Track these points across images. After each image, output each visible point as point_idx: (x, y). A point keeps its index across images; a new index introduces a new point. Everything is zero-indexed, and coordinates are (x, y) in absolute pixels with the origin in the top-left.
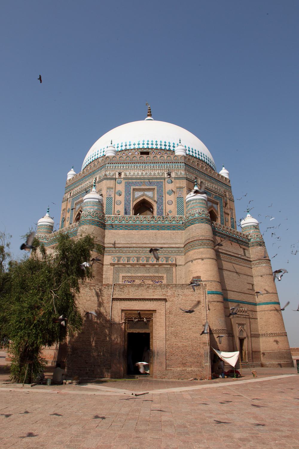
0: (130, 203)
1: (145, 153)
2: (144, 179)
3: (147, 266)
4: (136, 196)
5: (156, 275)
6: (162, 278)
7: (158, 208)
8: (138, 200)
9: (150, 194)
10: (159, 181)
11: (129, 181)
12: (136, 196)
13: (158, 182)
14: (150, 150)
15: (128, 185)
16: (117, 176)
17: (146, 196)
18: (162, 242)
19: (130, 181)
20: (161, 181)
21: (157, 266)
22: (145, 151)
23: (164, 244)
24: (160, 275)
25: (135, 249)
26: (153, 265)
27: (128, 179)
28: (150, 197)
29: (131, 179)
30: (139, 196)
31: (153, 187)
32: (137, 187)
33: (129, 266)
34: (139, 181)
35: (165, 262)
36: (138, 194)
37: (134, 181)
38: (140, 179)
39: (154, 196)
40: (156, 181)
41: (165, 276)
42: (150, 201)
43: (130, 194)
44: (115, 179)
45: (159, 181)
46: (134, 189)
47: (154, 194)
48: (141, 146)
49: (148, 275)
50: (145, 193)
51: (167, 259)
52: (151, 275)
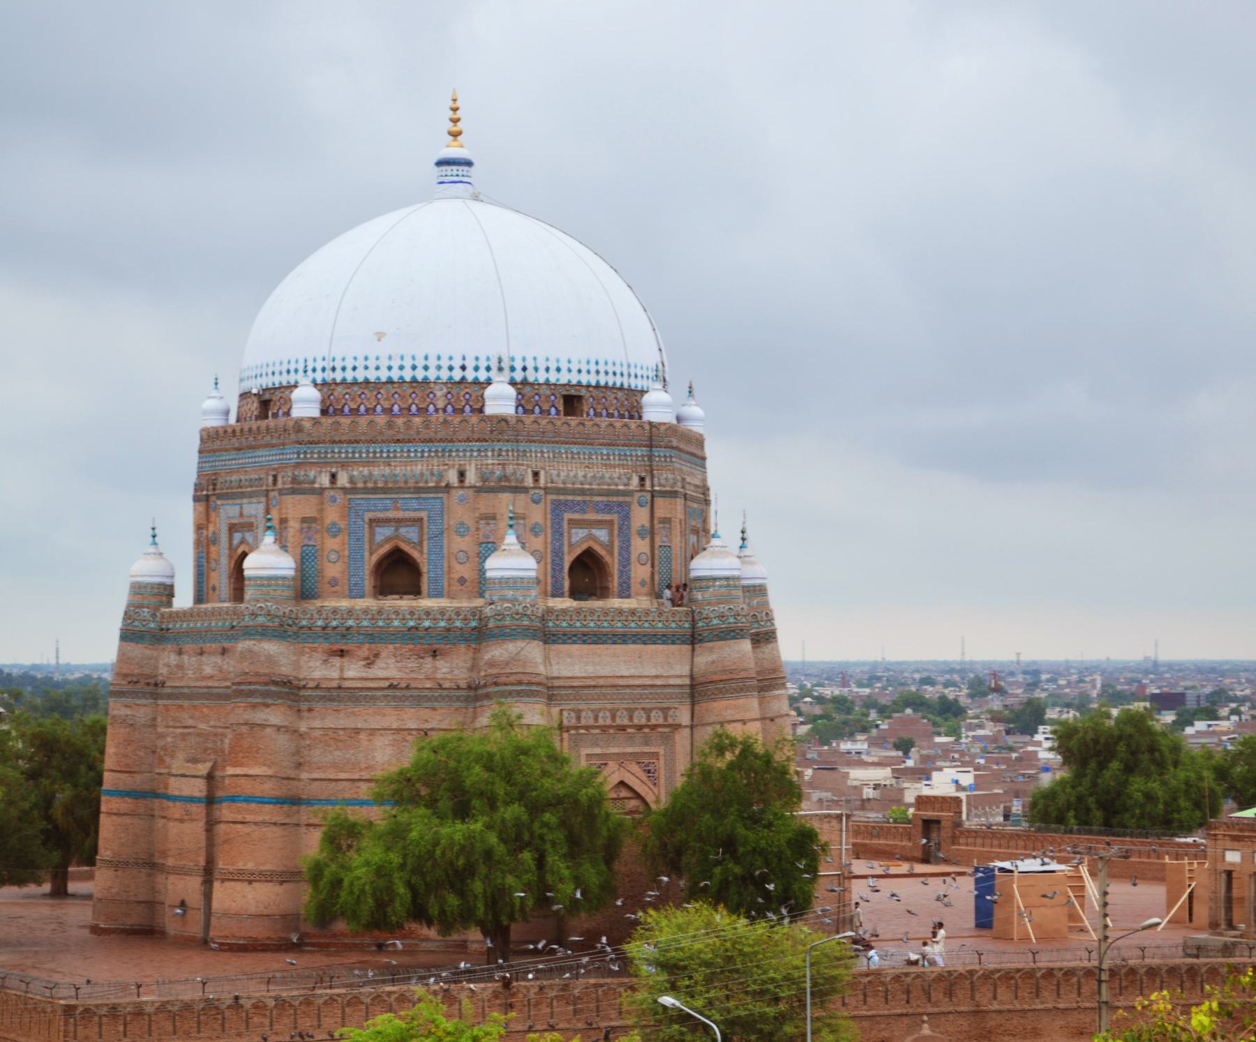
0: (562, 559)
1: (572, 401)
2: (591, 492)
3: (629, 730)
4: (574, 540)
5: (646, 749)
6: (655, 755)
7: (621, 573)
8: (578, 551)
9: (602, 534)
10: (621, 499)
11: (565, 502)
12: (574, 540)
13: (620, 504)
14: (583, 392)
15: (558, 508)
16: (529, 481)
17: (595, 539)
18: (653, 672)
19: (562, 497)
20: (627, 499)
21: (647, 730)
22: (573, 392)
23: (657, 677)
24: (653, 750)
25: (604, 691)
26: (640, 728)
27: (559, 491)
28: (601, 544)
29: (564, 491)
30: (578, 539)
31: (607, 517)
32: (577, 516)
33: (597, 731)
34: (579, 498)
35: (661, 721)
36: (579, 534)
37: (570, 498)
38: (582, 492)
39: (612, 542)
40: (615, 499)
41: (661, 751)
42: (602, 552)
43: (562, 535)
44: (525, 490)
45: (621, 499)
46: (571, 521)
47: (611, 534)
48: (564, 378)
49: (630, 750)
50: (594, 531)
51: (665, 711)
52: (637, 749)
